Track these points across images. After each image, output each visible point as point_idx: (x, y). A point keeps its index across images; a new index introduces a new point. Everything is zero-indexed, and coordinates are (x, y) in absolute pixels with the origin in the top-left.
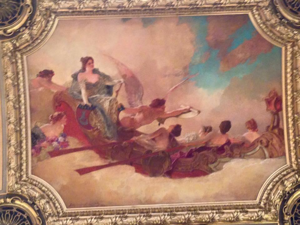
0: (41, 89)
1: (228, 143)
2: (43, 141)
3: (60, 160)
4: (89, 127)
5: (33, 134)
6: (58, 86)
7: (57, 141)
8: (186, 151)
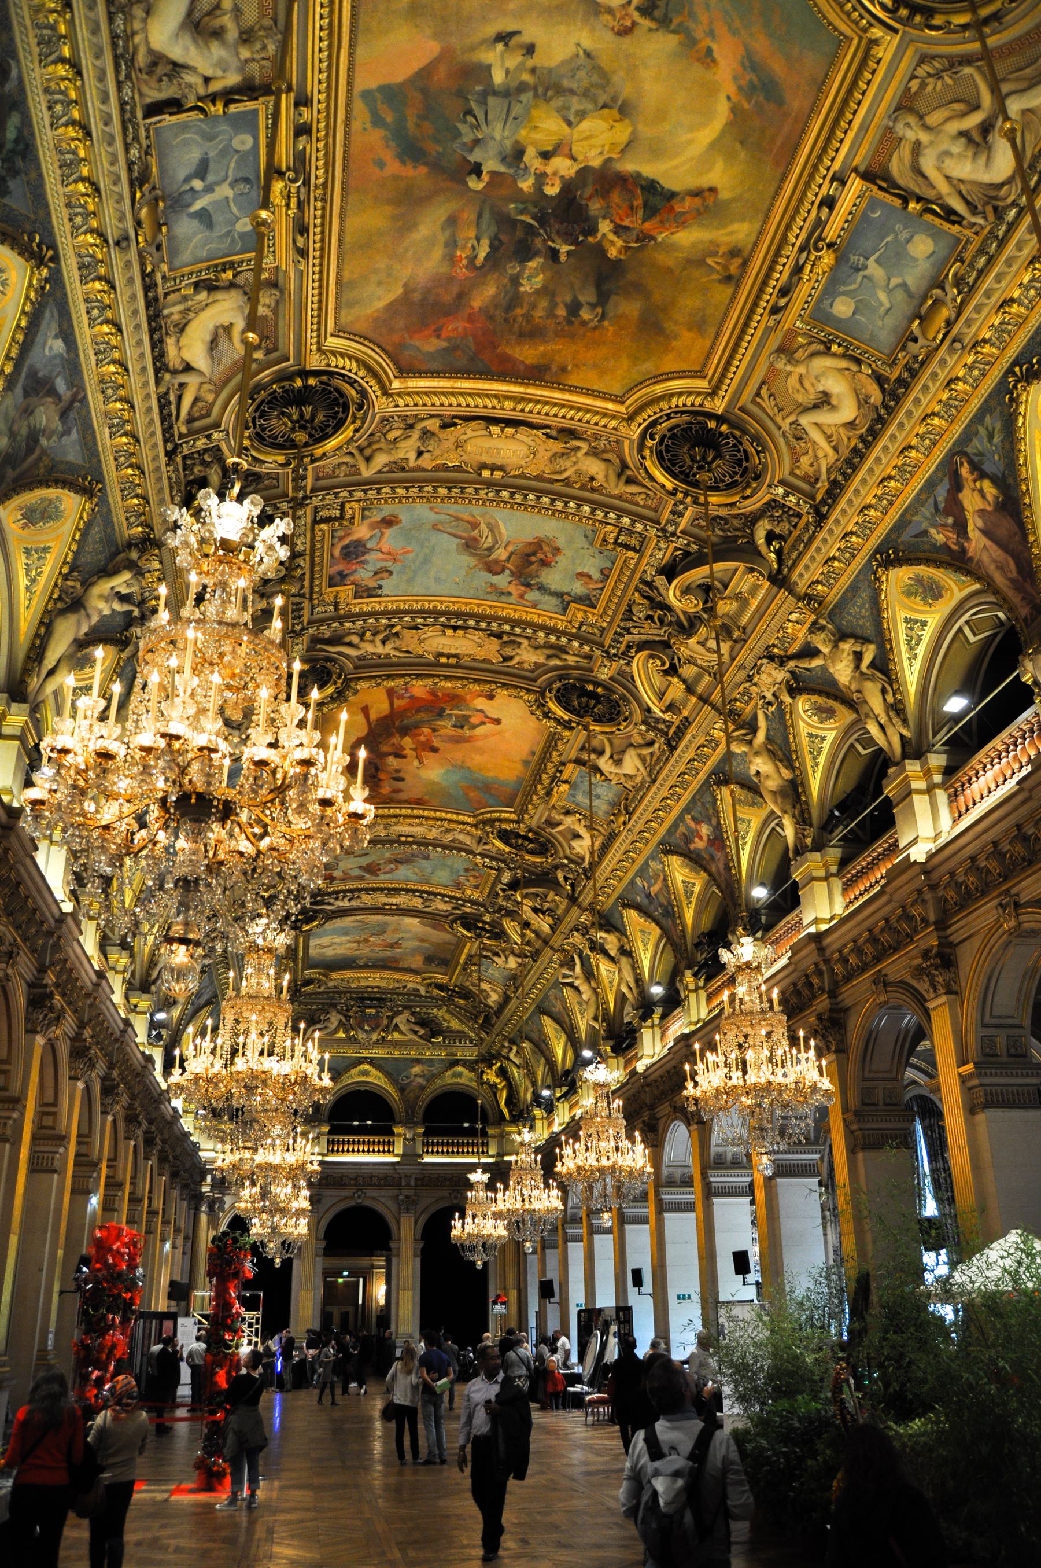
4: (418, 711)
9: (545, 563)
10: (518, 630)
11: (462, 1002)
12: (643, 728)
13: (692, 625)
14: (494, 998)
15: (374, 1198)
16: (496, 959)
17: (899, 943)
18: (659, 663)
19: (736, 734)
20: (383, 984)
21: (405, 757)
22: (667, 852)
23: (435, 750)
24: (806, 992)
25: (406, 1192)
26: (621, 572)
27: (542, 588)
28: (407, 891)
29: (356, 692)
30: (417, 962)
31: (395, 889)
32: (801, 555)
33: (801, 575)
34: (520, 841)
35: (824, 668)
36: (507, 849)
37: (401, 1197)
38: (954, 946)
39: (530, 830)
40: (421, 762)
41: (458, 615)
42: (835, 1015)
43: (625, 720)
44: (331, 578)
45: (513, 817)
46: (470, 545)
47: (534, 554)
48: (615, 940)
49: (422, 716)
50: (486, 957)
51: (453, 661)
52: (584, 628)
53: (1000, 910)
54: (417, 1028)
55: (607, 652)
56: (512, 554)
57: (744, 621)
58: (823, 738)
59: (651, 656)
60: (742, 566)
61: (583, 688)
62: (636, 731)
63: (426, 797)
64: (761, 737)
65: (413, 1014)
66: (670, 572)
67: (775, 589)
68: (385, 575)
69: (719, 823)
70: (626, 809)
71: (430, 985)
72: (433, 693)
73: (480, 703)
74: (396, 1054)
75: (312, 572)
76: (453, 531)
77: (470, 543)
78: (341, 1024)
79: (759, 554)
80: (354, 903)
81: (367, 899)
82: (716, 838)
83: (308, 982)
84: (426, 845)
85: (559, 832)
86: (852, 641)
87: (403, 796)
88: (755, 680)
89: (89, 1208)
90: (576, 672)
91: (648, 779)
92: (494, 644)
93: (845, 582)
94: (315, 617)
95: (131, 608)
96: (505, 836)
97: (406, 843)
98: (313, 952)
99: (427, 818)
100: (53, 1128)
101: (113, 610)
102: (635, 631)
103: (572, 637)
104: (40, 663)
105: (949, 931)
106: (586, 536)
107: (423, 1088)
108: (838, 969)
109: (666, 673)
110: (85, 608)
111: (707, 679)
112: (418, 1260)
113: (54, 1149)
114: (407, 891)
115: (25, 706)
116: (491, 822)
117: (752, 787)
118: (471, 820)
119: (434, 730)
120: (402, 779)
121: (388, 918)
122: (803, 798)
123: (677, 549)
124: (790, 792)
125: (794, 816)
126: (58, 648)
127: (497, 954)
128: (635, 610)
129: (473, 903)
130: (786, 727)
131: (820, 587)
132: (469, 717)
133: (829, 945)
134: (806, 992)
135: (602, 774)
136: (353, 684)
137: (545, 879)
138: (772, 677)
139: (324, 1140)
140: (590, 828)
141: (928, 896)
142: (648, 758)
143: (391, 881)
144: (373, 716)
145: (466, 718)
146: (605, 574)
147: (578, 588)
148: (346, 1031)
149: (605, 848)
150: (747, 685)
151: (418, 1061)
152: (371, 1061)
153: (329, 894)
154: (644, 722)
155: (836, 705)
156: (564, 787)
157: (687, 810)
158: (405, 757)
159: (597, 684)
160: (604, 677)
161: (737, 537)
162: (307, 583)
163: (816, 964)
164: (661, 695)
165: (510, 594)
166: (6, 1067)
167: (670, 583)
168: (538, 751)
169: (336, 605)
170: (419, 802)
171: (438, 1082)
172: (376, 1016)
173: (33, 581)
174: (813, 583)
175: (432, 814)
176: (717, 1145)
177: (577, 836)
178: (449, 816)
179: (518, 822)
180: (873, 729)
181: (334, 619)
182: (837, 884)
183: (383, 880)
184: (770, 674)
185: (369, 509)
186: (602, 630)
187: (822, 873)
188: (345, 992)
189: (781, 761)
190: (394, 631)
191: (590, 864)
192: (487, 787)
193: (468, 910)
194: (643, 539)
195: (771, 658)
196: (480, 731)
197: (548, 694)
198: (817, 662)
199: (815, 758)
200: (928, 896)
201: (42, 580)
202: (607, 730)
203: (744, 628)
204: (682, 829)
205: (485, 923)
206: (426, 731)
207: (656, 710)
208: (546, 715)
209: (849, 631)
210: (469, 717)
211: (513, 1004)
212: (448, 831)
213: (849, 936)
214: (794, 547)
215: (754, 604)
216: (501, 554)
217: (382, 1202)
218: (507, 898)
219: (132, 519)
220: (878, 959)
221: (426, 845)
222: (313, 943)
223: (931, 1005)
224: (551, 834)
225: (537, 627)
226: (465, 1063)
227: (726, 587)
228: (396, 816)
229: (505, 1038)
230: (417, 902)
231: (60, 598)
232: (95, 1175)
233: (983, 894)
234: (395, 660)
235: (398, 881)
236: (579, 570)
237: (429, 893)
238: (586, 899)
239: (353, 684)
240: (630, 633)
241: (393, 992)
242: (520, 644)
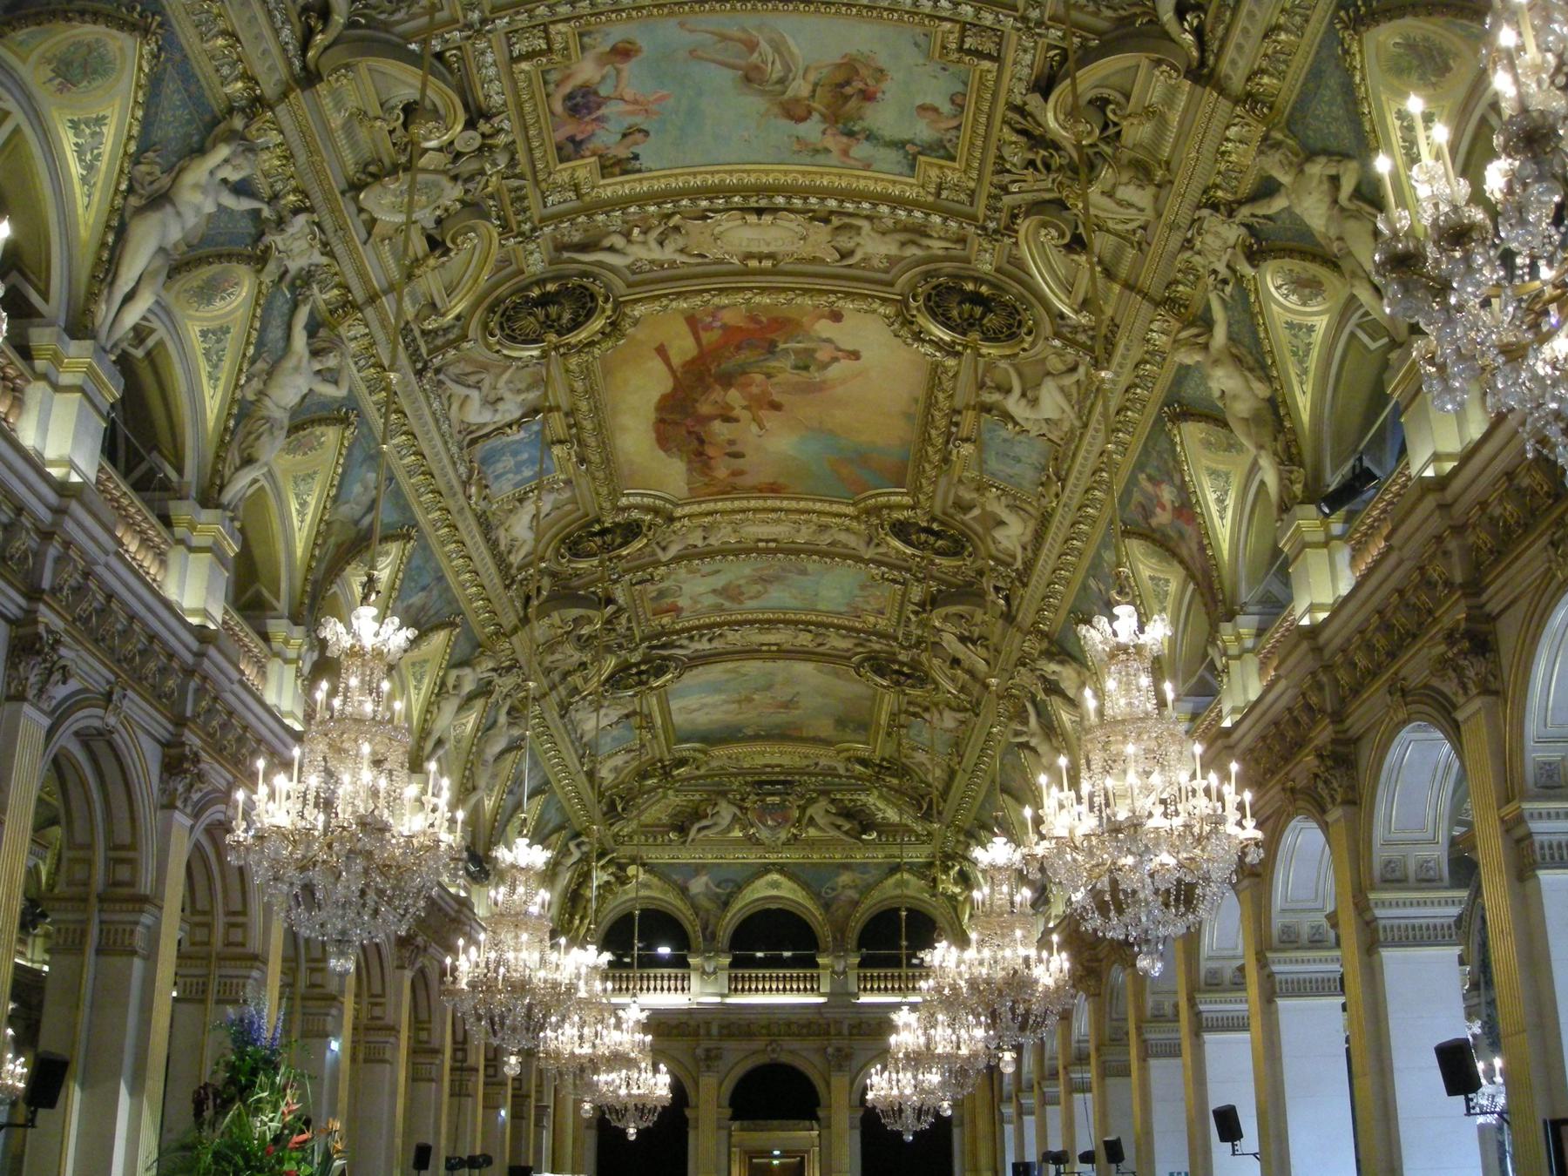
4: (739, 348)
9: (867, 96)
10: (849, 206)
11: (895, 781)
12: (1057, 343)
13: (1092, 167)
14: (937, 774)
15: (791, 1052)
16: (927, 716)
17: (1420, 625)
18: (1054, 233)
19: (1184, 334)
20: (786, 761)
21: (736, 420)
22: (1126, 534)
23: (776, 406)
24: (1304, 719)
25: (836, 1042)
26: (979, 97)
27: (870, 136)
28: (787, 622)
29: (636, 322)
30: (825, 728)
31: (769, 621)
32: (1228, 30)
33: (1233, 62)
34: (923, 537)
35: (1288, 210)
36: (909, 551)
37: (830, 1050)
38: (1492, 619)
39: (933, 519)
40: (761, 427)
41: (761, 190)
42: (1340, 749)
43: (1029, 333)
44: (559, 148)
45: (907, 500)
46: (751, 78)
47: (848, 83)
48: (1073, 675)
49: (744, 356)
50: (915, 715)
51: (767, 264)
52: (944, 194)
53: (1551, 550)
54: (839, 821)
55: (984, 228)
56: (816, 85)
57: (1166, 152)
58: (1311, 329)
59: (1044, 225)
60: (1143, 60)
61: (962, 291)
62: (1049, 350)
63: (781, 480)
64: (1220, 335)
65: (833, 801)
66: (1044, 86)
67: (1199, 89)
68: (639, 136)
69: (1183, 481)
70: (1057, 474)
71: (848, 759)
72: (753, 319)
73: (824, 328)
74: (816, 857)
75: (528, 139)
76: (720, 58)
77: (753, 75)
78: (735, 819)
79: (1166, 36)
80: (715, 644)
81: (734, 638)
82: (1183, 506)
83: (682, 762)
84: (797, 552)
85: (974, 519)
86: (1323, 160)
87: (748, 480)
88: (1198, 245)
89: (328, 1054)
90: (948, 267)
91: (1077, 423)
92: (821, 233)
93: (1300, 65)
94: (550, 210)
95: (256, 205)
96: (901, 530)
97: (767, 551)
98: (678, 719)
99: (787, 511)
100: (243, 945)
101: (219, 205)
102: (1014, 188)
103: (929, 209)
104: (112, 284)
105: (1485, 597)
106: (916, 44)
107: (856, 904)
108: (1343, 676)
109: (1069, 248)
110: (173, 204)
111: (1131, 253)
112: (857, 1135)
113: (243, 972)
114: (787, 622)
115: (88, 343)
116: (876, 510)
117: (1215, 417)
118: (850, 510)
119: (769, 376)
120: (737, 455)
121: (770, 664)
122: (1287, 424)
123: (1051, 47)
124: (1269, 417)
125: (1275, 453)
126: (136, 261)
127: (927, 709)
128: (1006, 152)
129: (881, 635)
130: (1253, 316)
131: (1266, 80)
132: (814, 351)
133: (1327, 644)
134: (1304, 719)
135: (1016, 423)
136: (628, 310)
137: (968, 592)
138: (1223, 235)
139: (723, 977)
140: (1012, 508)
141: (1452, 545)
142: (1074, 390)
143: (763, 610)
144: (676, 361)
145: (810, 353)
146: (958, 103)
147: (923, 131)
148: (743, 828)
149: (1039, 537)
150: (1187, 254)
151: (846, 867)
152: (781, 869)
153: (678, 632)
154: (1057, 335)
155: (1314, 269)
156: (967, 449)
157: (1140, 466)
158: (736, 420)
159: (978, 280)
160: (987, 267)
161: (1135, 15)
162: (521, 156)
163: (1313, 674)
164: (1068, 288)
165: (827, 151)
166: (131, 854)
167: (1046, 99)
168: (921, 393)
169: (576, 188)
170: (774, 489)
171: (876, 895)
172: (782, 806)
173: (90, 168)
174: (1255, 73)
175: (794, 505)
176: (1210, 958)
177: (1001, 523)
178: (818, 506)
179: (913, 508)
180: (1365, 295)
181: (577, 212)
182: (1343, 554)
183: (751, 606)
184: (1217, 235)
185: (589, 33)
186: (972, 194)
187: (1319, 536)
188: (735, 775)
189: (1251, 370)
190: (671, 224)
191: (1024, 563)
192: (861, 458)
193: (877, 647)
194: (1000, 37)
195: (1215, 207)
196: (834, 371)
197: (913, 304)
198: (1278, 204)
199: (1301, 362)
200: (1452, 545)
201: (103, 165)
202: (1008, 352)
203: (1168, 163)
204: (1137, 497)
205: (902, 664)
206: (759, 378)
207: (1066, 310)
208: (918, 336)
209: (1319, 145)
210: (814, 351)
211: (960, 780)
212: (823, 528)
213: (1354, 624)
214: (1218, 19)
215: (1174, 119)
216: (800, 88)
217: (804, 1056)
218: (923, 624)
219: (225, 71)
220: (1392, 655)
221: (797, 552)
222: (675, 705)
223: (1460, 716)
224: (963, 523)
225: (877, 199)
226: (912, 868)
227: (1127, 97)
228: (743, 511)
229: (960, 830)
230: (805, 639)
231: (130, 190)
232: (334, 1012)
233: (1527, 528)
234: (684, 271)
235: (772, 610)
236: (919, 102)
237: (818, 625)
238: (1025, 616)
239: (628, 310)
240: (1008, 192)
241: (803, 772)
242: (859, 228)
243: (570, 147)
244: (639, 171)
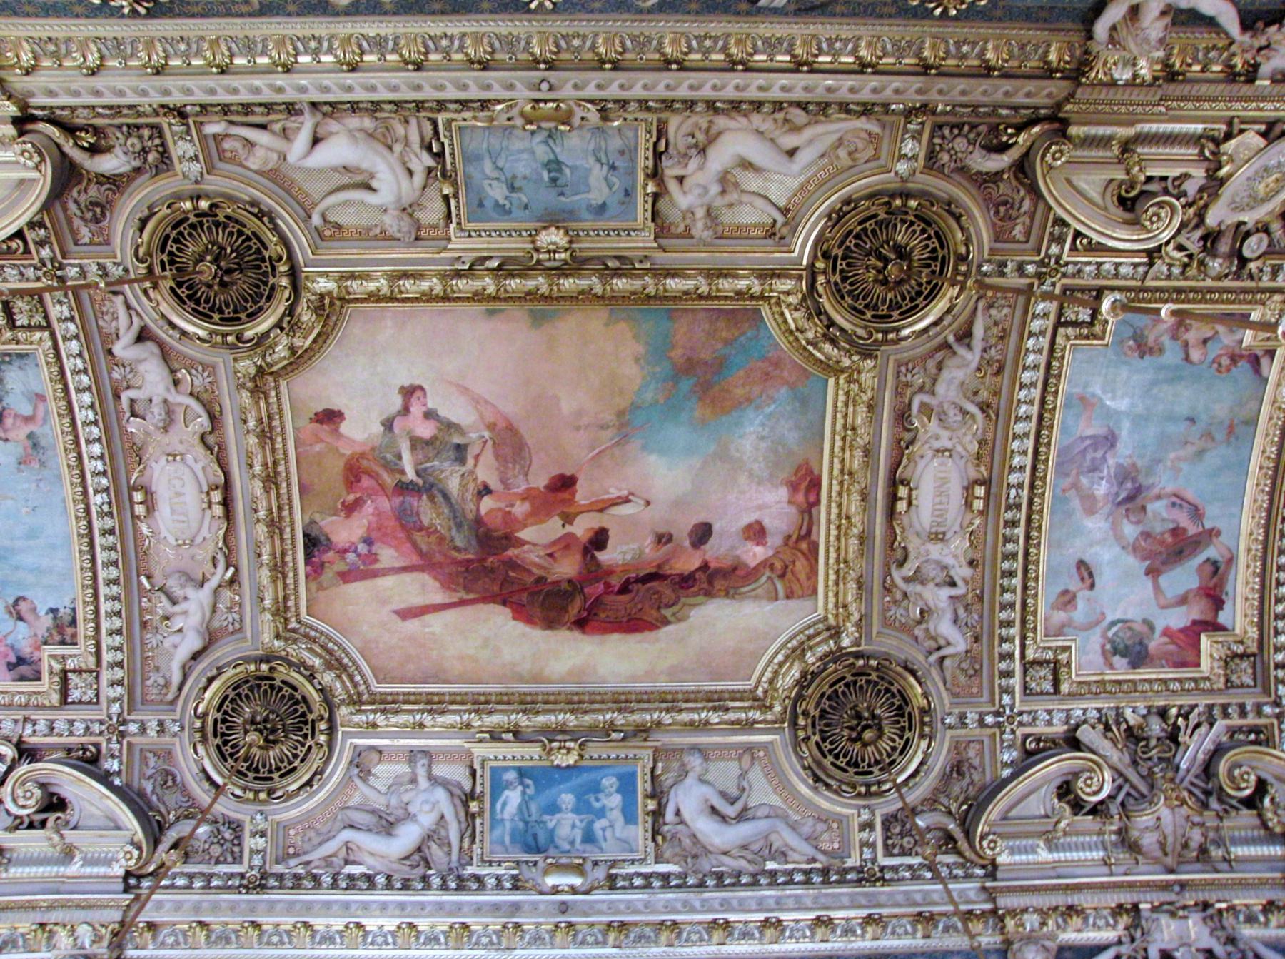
0: (318, 448)
1: (705, 567)
2: (326, 551)
3: (358, 589)
5: (306, 535)
6: (354, 441)
7: (355, 551)
8: (616, 581)
144: (439, 597)
165: (30, 436)
243: (23, 669)
244: (74, 610)
